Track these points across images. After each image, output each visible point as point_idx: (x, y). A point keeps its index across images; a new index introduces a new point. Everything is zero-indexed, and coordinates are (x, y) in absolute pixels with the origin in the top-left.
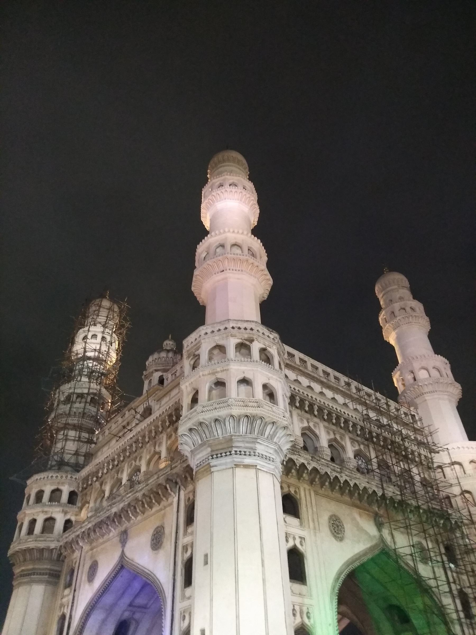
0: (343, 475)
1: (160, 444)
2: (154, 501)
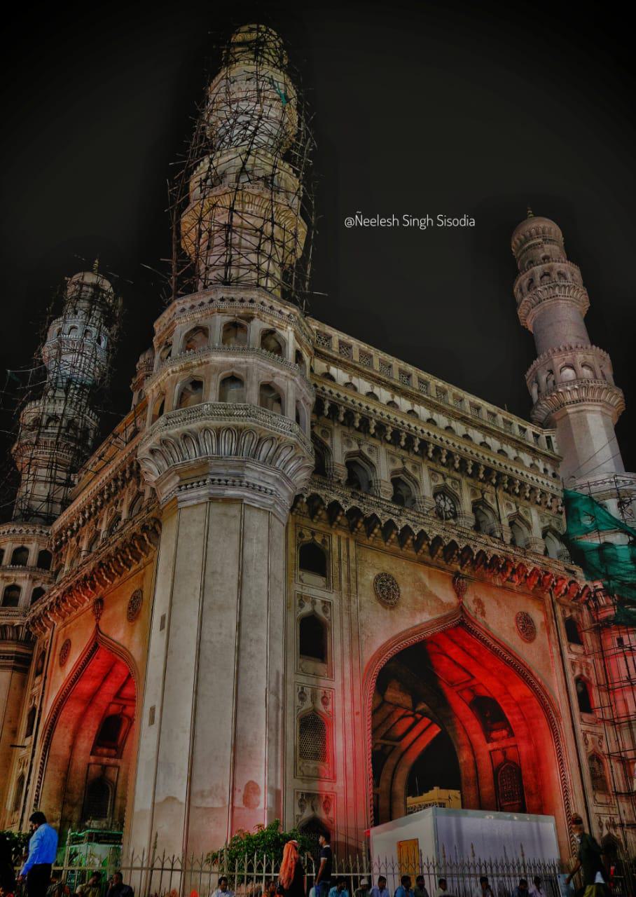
0: (401, 518)
2: (130, 557)
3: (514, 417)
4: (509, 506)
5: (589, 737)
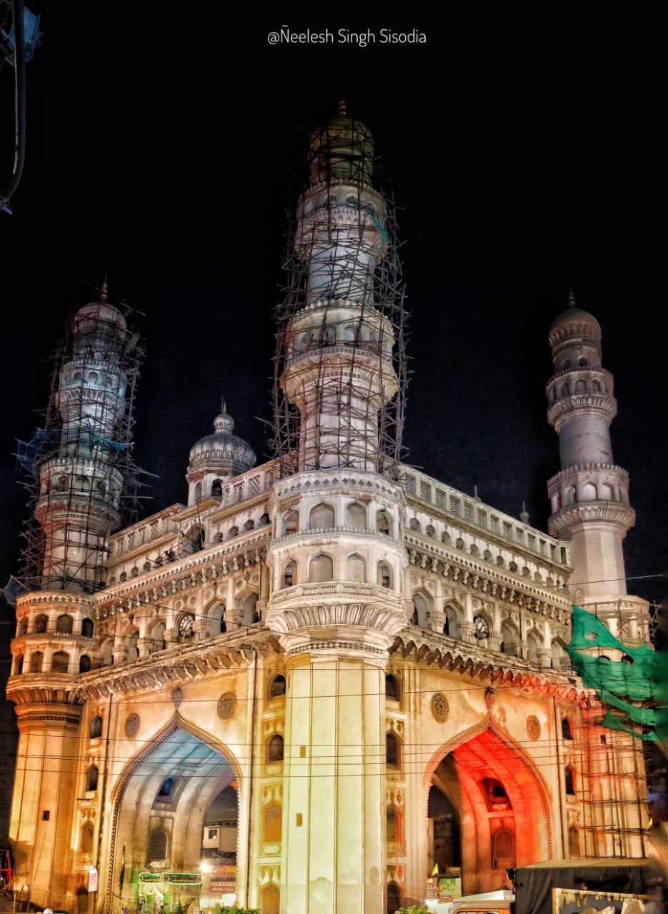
0: (456, 650)
1: (223, 590)
3: (537, 531)
4: (528, 622)
5: (571, 813)
